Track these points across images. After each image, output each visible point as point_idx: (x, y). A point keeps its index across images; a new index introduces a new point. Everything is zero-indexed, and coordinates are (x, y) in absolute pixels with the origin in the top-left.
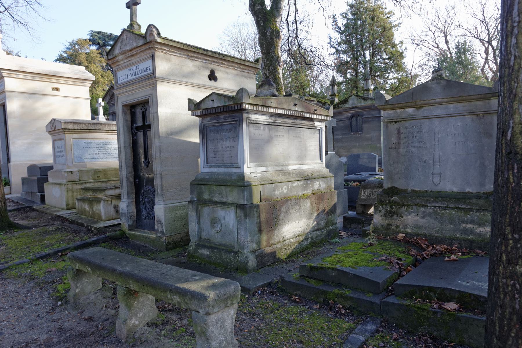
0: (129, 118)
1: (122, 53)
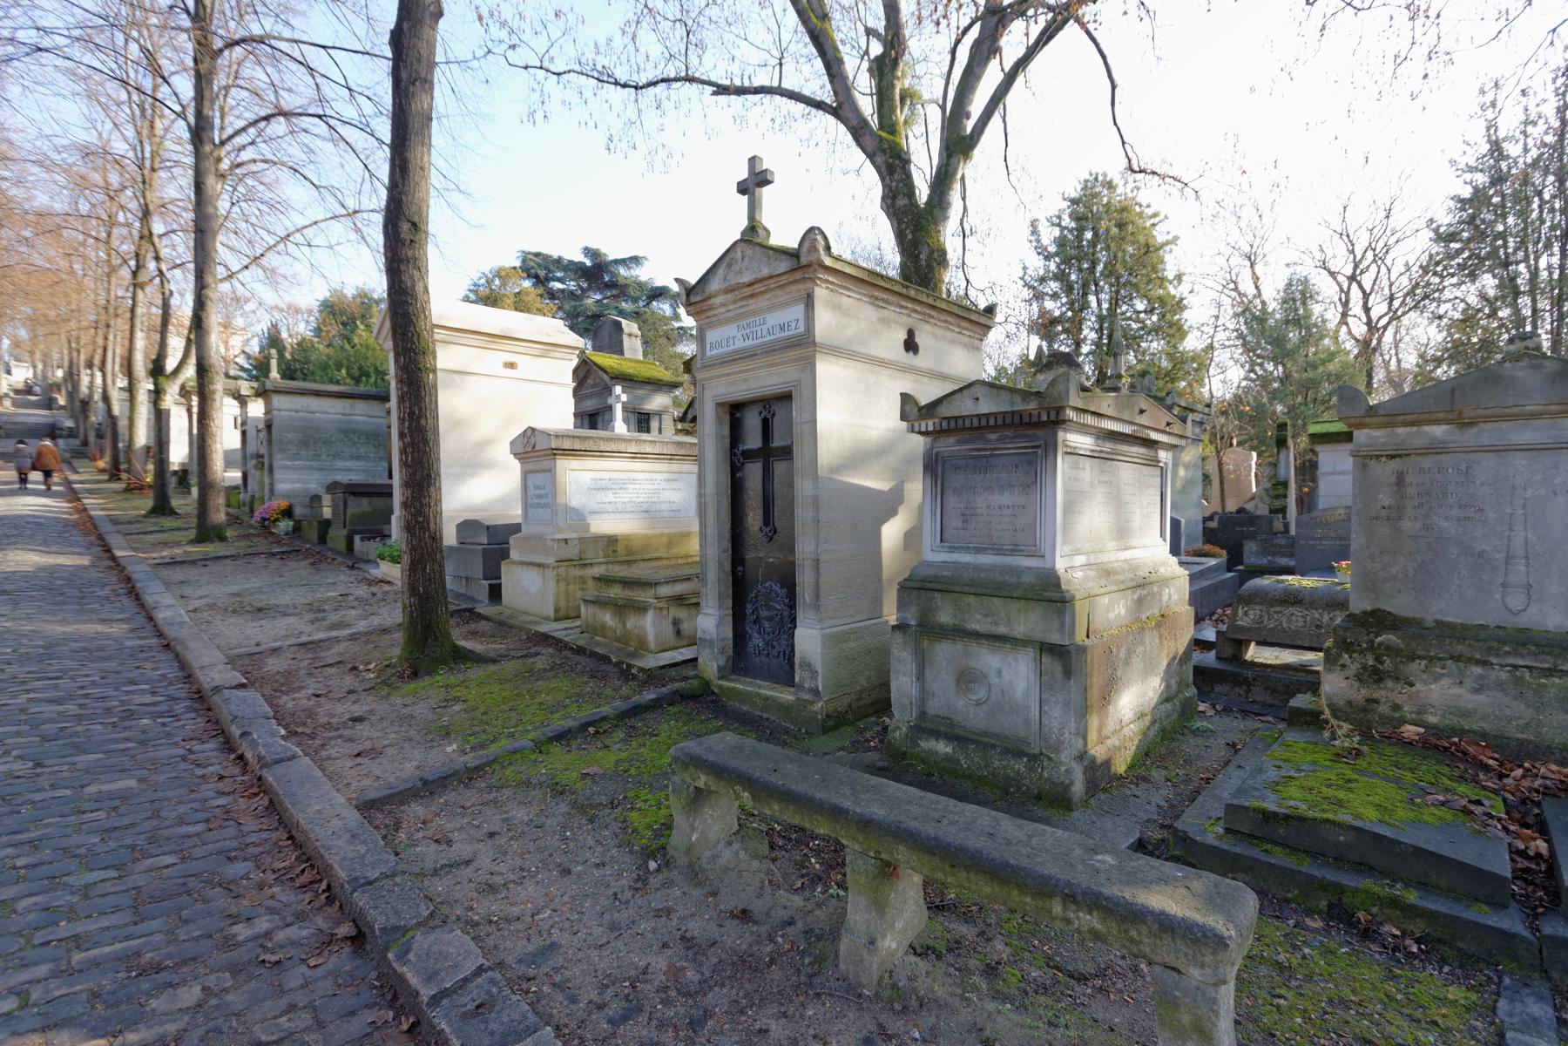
0: (726, 431)
1: (727, 291)
